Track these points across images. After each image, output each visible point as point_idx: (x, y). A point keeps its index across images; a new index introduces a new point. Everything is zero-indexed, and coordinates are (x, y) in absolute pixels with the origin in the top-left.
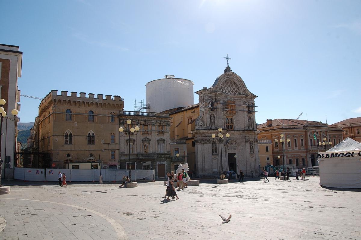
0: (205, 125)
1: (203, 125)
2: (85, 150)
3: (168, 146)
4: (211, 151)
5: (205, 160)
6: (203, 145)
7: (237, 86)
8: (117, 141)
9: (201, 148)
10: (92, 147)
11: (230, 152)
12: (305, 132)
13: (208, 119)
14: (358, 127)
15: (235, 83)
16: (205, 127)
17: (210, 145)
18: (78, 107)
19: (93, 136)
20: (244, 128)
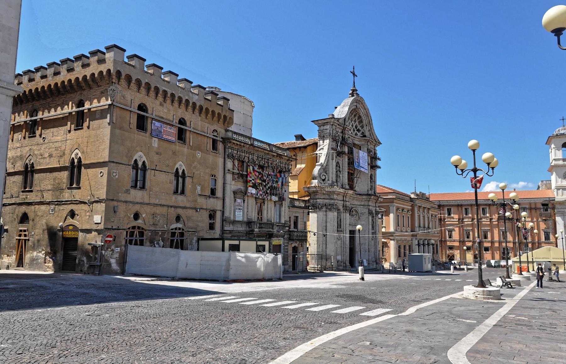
0: (331, 179)
1: (327, 179)
2: (168, 206)
3: (287, 209)
4: (336, 225)
7: (361, 122)
8: (219, 193)
10: (180, 200)
11: (351, 229)
12: (412, 206)
13: (335, 170)
14: (450, 205)
15: (360, 117)
16: (330, 182)
17: (336, 214)
18: (161, 104)
19: (184, 176)
20: (368, 191)
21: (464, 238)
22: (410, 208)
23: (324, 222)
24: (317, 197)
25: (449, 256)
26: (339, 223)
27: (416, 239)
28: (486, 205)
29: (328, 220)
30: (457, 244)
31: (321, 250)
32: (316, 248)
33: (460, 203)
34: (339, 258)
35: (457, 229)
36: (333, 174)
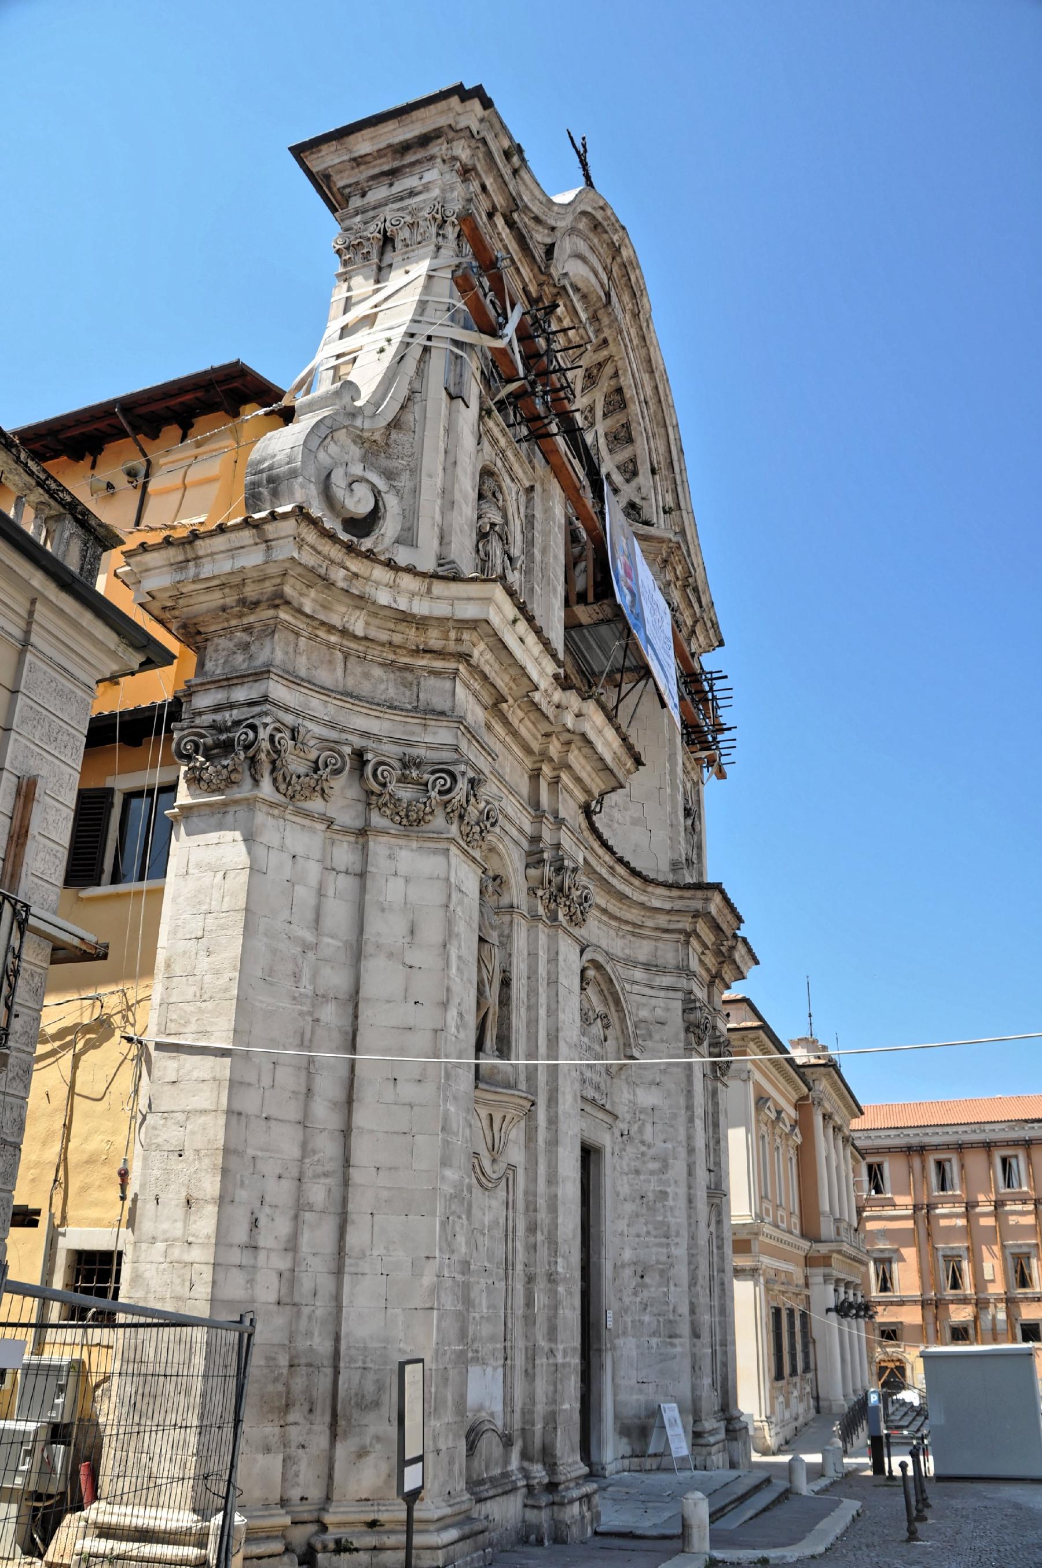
1: (389, 527)
5: (362, 1151)
6: (344, 854)
9: (305, 895)
12: (801, 1105)
14: (878, 1151)
21: (938, 1287)
22: (793, 1113)
23: (332, 945)
24: (275, 651)
25: (882, 1370)
26: (493, 995)
27: (827, 1278)
28: (1015, 1143)
29: (385, 928)
30: (911, 1316)
31: (267, 1290)
32: (202, 1255)
33: (914, 1141)
34: (485, 1390)
35: (910, 1253)
36: (449, 504)
